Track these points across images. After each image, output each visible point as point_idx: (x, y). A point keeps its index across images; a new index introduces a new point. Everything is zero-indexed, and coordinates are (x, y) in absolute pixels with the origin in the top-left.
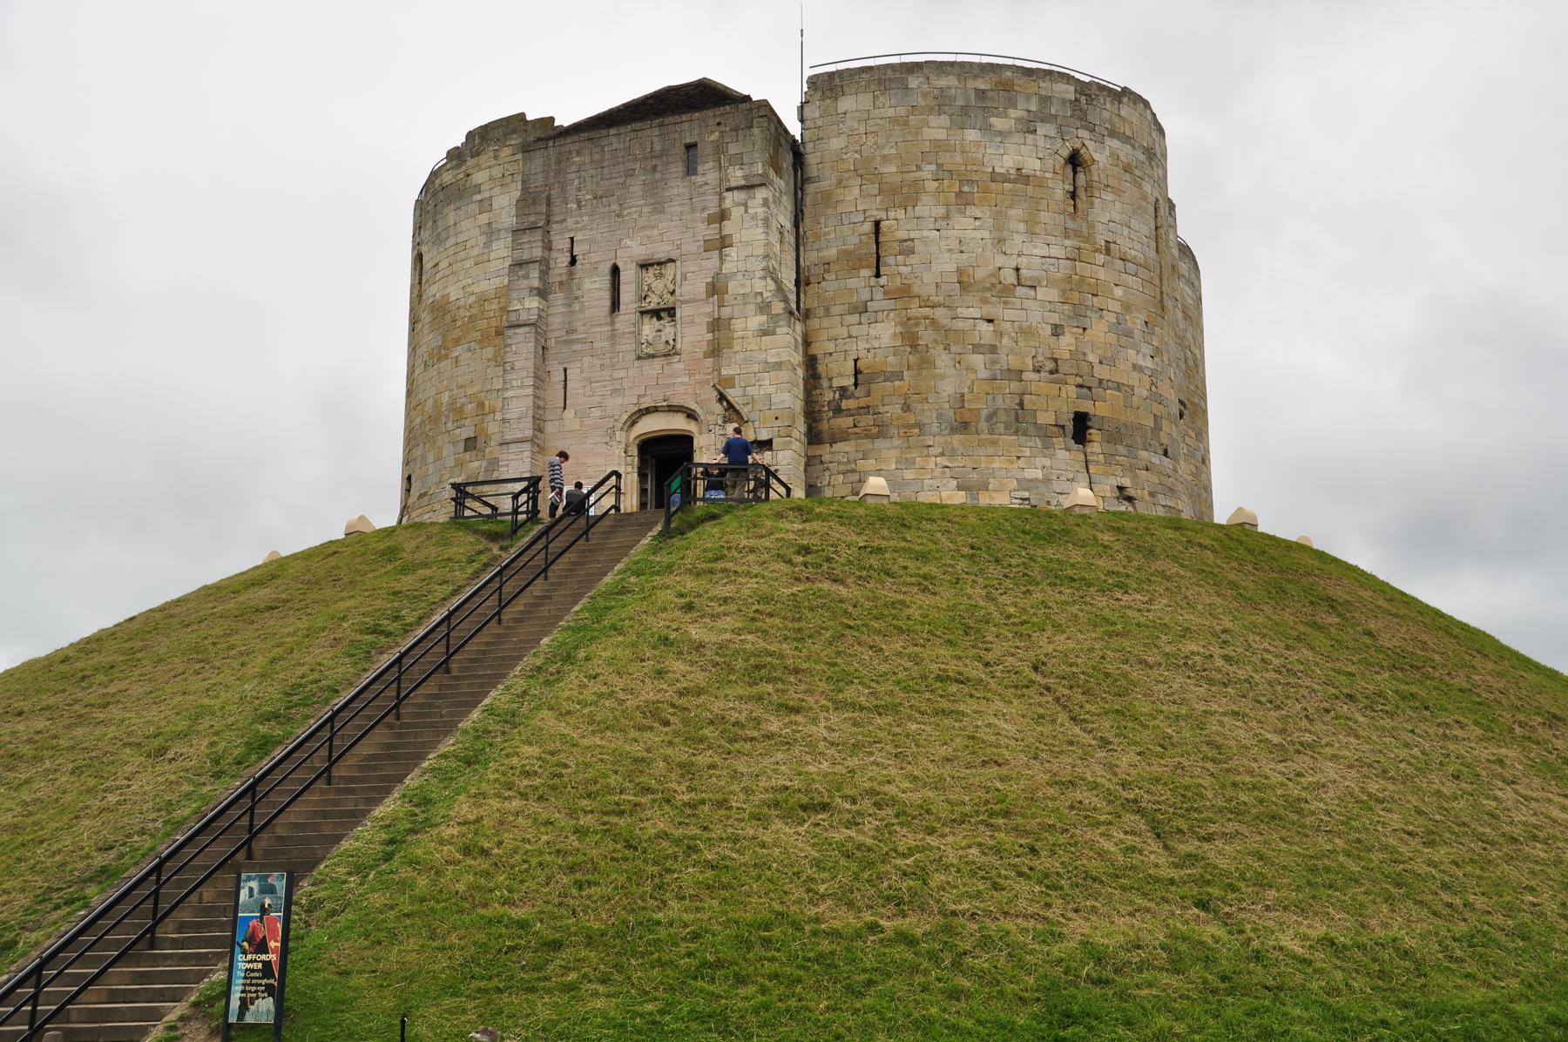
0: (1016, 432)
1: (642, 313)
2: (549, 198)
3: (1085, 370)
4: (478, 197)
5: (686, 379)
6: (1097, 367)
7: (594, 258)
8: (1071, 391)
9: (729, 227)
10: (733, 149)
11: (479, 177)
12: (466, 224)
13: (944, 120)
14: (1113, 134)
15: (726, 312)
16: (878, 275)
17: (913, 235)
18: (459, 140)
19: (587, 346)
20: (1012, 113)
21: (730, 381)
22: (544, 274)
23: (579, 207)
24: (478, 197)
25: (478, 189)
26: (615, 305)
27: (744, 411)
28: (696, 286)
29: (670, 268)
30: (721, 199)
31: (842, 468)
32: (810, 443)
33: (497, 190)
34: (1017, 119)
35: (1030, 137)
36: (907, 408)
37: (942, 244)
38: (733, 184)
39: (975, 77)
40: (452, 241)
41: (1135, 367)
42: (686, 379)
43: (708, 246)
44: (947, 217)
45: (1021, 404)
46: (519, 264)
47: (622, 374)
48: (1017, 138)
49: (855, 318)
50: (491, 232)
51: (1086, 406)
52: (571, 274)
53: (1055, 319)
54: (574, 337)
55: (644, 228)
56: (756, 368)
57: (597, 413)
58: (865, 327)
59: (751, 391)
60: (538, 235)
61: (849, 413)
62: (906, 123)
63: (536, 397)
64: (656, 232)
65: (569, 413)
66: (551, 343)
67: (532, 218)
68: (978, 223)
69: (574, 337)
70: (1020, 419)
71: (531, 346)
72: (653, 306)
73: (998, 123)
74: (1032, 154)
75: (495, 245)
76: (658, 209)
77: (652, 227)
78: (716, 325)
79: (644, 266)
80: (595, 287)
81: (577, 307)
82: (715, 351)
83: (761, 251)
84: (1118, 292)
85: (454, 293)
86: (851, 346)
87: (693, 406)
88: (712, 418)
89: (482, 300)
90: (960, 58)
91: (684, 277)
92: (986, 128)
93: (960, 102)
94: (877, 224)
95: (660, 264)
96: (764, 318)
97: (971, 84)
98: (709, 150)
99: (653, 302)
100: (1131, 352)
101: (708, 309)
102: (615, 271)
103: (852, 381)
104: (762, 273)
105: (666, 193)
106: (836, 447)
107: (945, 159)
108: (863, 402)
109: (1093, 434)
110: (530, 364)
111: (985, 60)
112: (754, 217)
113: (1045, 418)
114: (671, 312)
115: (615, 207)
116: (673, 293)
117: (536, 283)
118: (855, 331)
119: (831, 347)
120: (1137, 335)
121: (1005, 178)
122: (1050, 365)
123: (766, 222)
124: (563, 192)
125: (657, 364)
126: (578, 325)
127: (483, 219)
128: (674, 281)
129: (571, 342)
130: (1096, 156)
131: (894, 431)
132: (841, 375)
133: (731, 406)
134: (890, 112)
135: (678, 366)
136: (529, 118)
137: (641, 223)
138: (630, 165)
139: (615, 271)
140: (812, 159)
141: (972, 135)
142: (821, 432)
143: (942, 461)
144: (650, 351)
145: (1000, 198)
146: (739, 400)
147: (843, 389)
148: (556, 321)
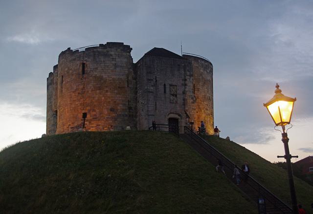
9: (187, 82)
10: (188, 68)
15: (186, 98)
18: (105, 43)
24: (111, 57)
25: (111, 55)
28: (180, 91)
29: (175, 87)
33: (117, 57)
50: (116, 66)
52: (157, 84)
57: (162, 112)
65: (157, 111)
78: (184, 100)
79: (171, 85)
82: (184, 104)
85: (105, 76)
89: (114, 79)
92: (207, 72)
99: (172, 93)
114: (176, 96)
127: (114, 62)
133: (187, 115)
136: (124, 44)
137: (170, 77)
139: (165, 85)
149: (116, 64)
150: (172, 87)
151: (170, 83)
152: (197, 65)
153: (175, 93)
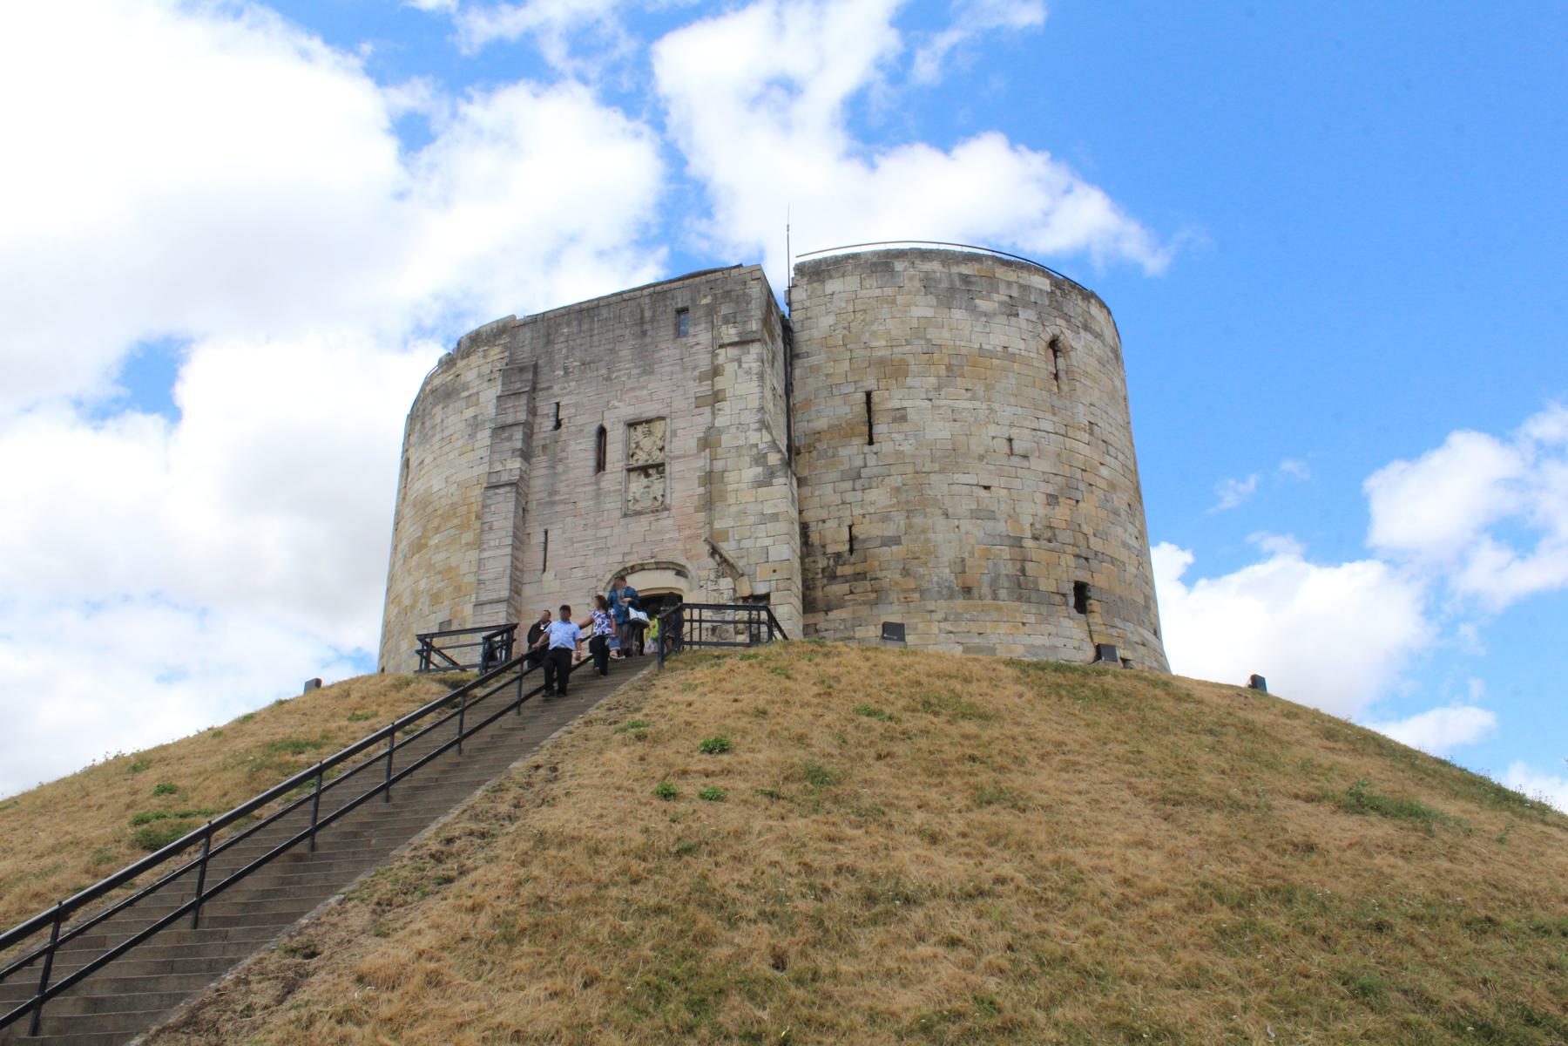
0: (1020, 599)
1: (629, 470)
2: (536, 367)
3: (1082, 542)
4: (466, 394)
5: (675, 535)
6: (1092, 540)
7: (580, 420)
8: (1068, 560)
9: (721, 383)
10: (725, 309)
11: (470, 376)
12: (454, 419)
13: (932, 300)
14: (1086, 328)
15: (719, 465)
16: (871, 442)
17: (905, 404)
19: (571, 506)
20: (995, 297)
21: (724, 535)
22: (529, 436)
23: (566, 373)
24: (466, 394)
25: (465, 387)
26: (600, 466)
27: (741, 564)
28: (685, 439)
29: (658, 428)
30: (714, 355)
31: (839, 635)
32: (805, 611)
34: (1001, 303)
35: (1013, 319)
36: (906, 572)
37: (925, 417)
38: (726, 341)
39: (958, 264)
40: (438, 436)
41: (1124, 545)
42: (675, 535)
43: (700, 402)
44: (939, 388)
45: (1023, 571)
46: (500, 429)
47: (607, 532)
48: (1002, 319)
49: (848, 485)
51: (1083, 576)
53: (1050, 489)
54: (557, 498)
55: (633, 389)
56: (751, 519)
57: (579, 573)
58: (859, 493)
59: (745, 544)
60: (524, 400)
61: (845, 579)
62: (894, 302)
63: (514, 558)
64: (645, 392)
65: (549, 575)
66: (533, 505)
67: (518, 385)
68: (969, 394)
69: (557, 498)
70: (1022, 588)
71: (511, 506)
72: (641, 463)
73: (983, 305)
74: (1015, 337)
75: (480, 435)
76: (648, 370)
77: (642, 388)
79: (632, 425)
80: (581, 451)
81: (560, 468)
82: (709, 504)
83: (756, 405)
84: (1104, 471)
85: (436, 484)
86: (845, 513)
87: (682, 561)
88: (704, 574)
90: (942, 247)
91: (674, 434)
92: (972, 310)
93: (945, 285)
94: (868, 395)
95: (648, 421)
96: (760, 469)
97: (955, 270)
98: (701, 313)
99: (641, 459)
100: (1120, 530)
101: (701, 463)
102: (602, 432)
103: (847, 547)
104: (757, 426)
105: (657, 355)
106: (832, 615)
107: (932, 333)
108: (859, 568)
109: (1093, 604)
110: (510, 524)
111: (966, 250)
112: (748, 372)
113: (1046, 585)
114: (659, 467)
115: (603, 371)
116: (662, 449)
117: (519, 445)
118: (849, 497)
119: (823, 514)
120: (1123, 513)
121: (991, 354)
122: (1049, 534)
123: (761, 377)
124: (551, 361)
125: (644, 521)
126: (562, 487)
127: (469, 413)
128: (663, 438)
129: (553, 503)
130: (1074, 344)
131: (893, 596)
132: (836, 542)
134: (878, 292)
135: (666, 522)
137: (628, 386)
138: (618, 332)
139: (602, 432)
140: (801, 336)
141: (958, 314)
142: (815, 599)
143: (947, 626)
144: (638, 507)
145: (989, 373)
146: (733, 554)
147: (838, 555)
148: (538, 484)
149: (475, 417)
150: (639, 428)
151: (629, 411)
152: (889, 291)
153: (658, 457)
